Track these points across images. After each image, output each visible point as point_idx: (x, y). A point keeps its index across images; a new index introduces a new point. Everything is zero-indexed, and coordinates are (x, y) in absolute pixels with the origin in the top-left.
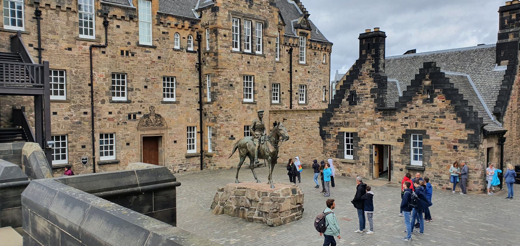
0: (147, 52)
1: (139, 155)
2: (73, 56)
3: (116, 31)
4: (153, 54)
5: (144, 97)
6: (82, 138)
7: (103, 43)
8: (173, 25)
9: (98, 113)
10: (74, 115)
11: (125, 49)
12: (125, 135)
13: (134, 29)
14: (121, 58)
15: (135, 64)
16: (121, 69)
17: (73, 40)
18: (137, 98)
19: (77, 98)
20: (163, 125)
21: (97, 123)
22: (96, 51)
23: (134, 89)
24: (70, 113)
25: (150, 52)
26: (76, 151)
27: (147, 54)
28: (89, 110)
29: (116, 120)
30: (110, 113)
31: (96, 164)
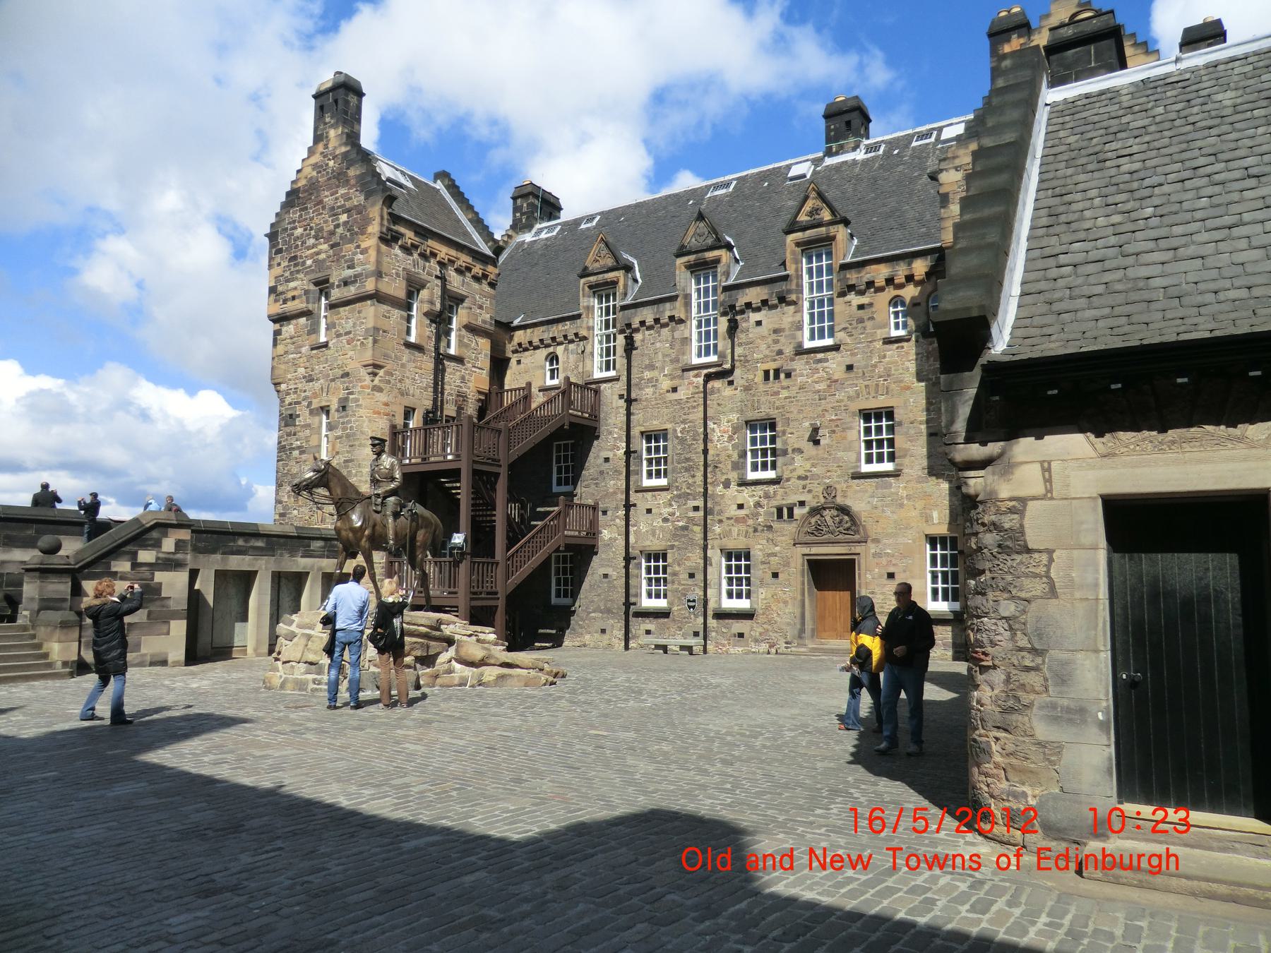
0: (820, 361)
1: (798, 603)
2: (679, 402)
3: (755, 332)
4: (834, 364)
5: (813, 465)
6: (688, 559)
7: (727, 366)
8: (880, 282)
9: (717, 508)
10: (678, 514)
11: (771, 366)
12: (769, 555)
13: (790, 319)
14: (762, 387)
15: (793, 393)
16: (764, 411)
17: (680, 372)
18: (794, 470)
19: (683, 478)
20: (857, 532)
21: (718, 529)
22: (716, 384)
23: (790, 450)
24: (670, 510)
25: (826, 360)
26: (680, 584)
27: (819, 365)
28: (700, 503)
29: (750, 522)
30: (741, 506)
31: (710, 613)
